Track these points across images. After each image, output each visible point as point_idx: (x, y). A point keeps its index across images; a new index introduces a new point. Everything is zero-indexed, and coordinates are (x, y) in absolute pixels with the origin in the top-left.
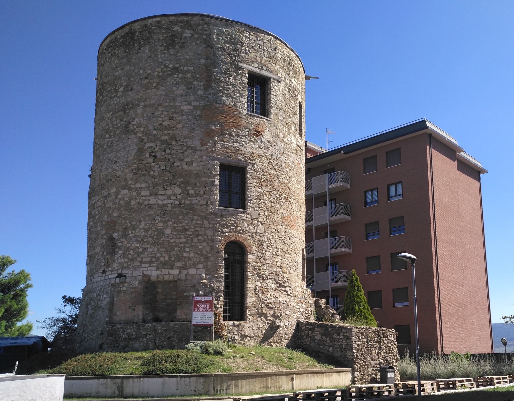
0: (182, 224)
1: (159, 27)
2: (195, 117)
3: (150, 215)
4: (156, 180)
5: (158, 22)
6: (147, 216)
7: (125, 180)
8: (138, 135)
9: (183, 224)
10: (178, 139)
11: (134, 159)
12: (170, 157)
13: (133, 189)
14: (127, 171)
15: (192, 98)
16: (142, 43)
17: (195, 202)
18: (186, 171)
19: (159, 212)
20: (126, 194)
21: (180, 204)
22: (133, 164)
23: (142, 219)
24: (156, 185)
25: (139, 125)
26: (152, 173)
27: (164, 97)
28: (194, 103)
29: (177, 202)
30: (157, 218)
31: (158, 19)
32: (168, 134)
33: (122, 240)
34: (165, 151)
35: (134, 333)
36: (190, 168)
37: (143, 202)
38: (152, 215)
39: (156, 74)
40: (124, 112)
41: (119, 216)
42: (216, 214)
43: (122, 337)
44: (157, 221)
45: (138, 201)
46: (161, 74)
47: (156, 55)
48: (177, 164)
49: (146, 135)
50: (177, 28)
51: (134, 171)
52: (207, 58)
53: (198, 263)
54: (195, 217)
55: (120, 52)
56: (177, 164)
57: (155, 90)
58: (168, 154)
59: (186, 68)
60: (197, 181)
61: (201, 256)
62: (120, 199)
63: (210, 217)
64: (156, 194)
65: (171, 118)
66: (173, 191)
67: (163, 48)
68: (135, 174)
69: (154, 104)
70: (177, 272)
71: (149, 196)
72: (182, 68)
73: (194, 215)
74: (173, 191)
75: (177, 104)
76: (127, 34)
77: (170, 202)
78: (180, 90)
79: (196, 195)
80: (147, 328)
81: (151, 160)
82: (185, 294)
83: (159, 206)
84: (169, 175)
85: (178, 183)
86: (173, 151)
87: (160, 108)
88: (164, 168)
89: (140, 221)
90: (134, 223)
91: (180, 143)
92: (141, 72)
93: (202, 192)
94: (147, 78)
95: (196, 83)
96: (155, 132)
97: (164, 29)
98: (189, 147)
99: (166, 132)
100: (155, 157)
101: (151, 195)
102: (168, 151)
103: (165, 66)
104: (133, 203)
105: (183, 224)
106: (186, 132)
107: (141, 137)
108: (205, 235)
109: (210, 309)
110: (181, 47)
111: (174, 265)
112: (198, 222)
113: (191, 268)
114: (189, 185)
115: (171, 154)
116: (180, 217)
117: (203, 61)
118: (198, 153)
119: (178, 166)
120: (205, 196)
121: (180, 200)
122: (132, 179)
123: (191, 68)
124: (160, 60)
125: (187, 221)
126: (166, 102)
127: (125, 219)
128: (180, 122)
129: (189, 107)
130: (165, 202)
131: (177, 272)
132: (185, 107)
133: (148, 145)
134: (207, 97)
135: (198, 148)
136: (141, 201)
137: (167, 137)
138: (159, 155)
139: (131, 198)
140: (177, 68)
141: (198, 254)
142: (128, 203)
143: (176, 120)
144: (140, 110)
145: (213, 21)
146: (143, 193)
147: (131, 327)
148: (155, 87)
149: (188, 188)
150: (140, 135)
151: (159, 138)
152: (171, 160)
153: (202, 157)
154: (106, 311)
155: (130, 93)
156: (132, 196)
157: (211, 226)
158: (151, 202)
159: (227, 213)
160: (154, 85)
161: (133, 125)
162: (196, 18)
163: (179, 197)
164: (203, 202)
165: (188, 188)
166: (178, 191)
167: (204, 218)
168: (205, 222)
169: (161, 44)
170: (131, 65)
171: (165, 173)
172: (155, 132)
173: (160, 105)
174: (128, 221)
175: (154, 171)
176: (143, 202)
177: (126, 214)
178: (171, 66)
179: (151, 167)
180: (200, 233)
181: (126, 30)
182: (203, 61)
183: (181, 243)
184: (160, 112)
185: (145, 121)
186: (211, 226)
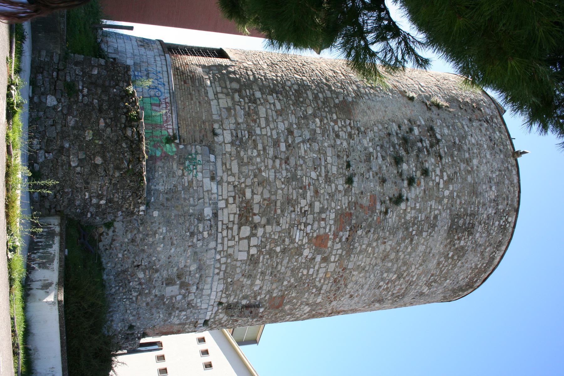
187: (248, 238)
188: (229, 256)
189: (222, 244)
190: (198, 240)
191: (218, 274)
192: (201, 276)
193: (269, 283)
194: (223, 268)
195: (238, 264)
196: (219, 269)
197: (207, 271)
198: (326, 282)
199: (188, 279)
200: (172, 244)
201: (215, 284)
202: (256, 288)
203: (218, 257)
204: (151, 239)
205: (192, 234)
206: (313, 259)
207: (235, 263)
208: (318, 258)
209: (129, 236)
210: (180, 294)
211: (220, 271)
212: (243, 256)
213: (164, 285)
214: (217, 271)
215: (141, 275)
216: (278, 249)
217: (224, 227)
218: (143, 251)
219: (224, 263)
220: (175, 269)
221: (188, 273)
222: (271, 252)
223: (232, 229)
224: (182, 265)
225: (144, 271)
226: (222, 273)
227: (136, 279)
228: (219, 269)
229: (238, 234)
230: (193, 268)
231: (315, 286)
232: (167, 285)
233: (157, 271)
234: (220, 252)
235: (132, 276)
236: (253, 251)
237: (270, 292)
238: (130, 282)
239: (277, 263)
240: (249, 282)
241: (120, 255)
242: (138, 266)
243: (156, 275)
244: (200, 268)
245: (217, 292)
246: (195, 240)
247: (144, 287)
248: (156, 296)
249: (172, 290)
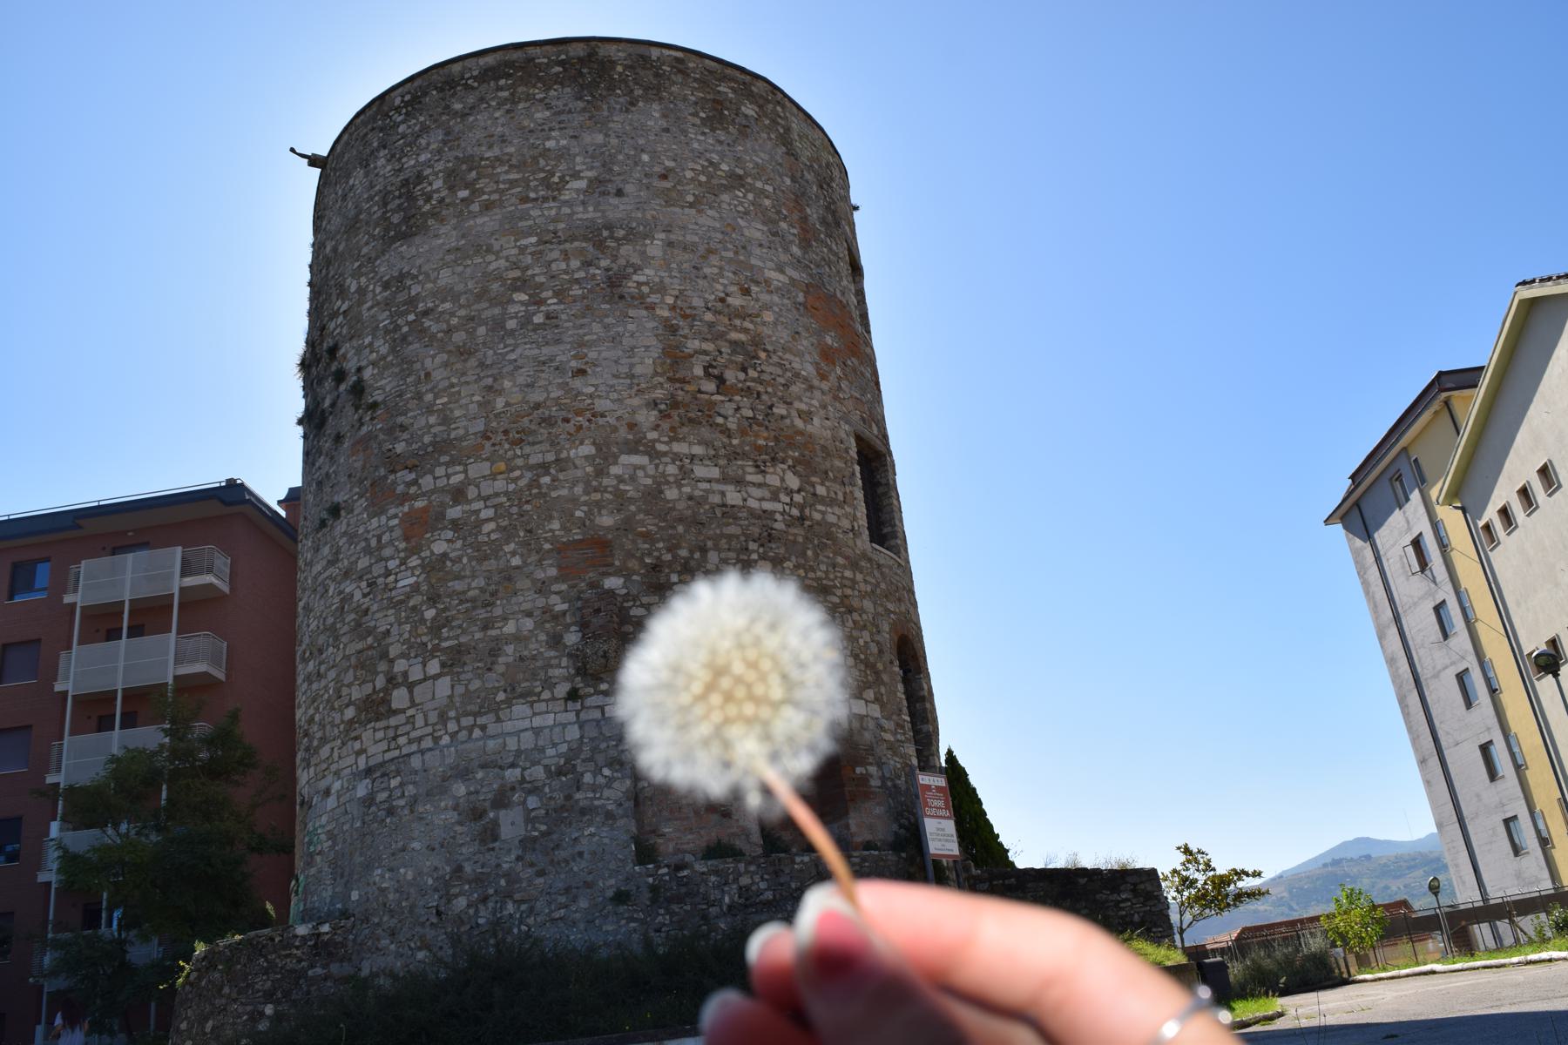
0: (814, 571)
1: (680, 71)
2: (797, 305)
3: (730, 537)
4: (735, 442)
5: (677, 59)
6: (722, 536)
7: (632, 426)
8: (658, 312)
10: (769, 348)
11: (656, 374)
12: (761, 388)
13: (665, 454)
14: (636, 401)
15: (784, 258)
16: (638, 92)
17: (831, 519)
18: (801, 433)
19: (756, 531)
20: (642, 468)
21: (802, 518)
22: (655, 387)
23: (710, 544)
24: (735, 455)
25: (661, 289)
26: (720, 420)
27: (720, 236)
28: (790, 271)
29: (795, 512)
30: (753, 546)
31: (679, 54)
32: (746, 331)
33: (645, 600)
34: (744, 370)
35: (763, 885)
36: (809, 427)
37: (705, 499)
38: (737, 537)
39: (689, 174)
40: (600, 245)
41: (627, 526)
43: (721, 900)
44: (754, 556)
45: (687, 490)
46: (703, 178)
47: (685, 132)
48: (780, 410)
49: (685, 317)
51: (663, 407)
52: (793, 180)
54: (840, 560)
55: (562, 96)
56: (780, 410)
57: (693, 211)
58: (753, 380)
59: (759, 184)
62: (620, 479)
64: (740, 482)
65: (746, 292)
66: (782, 480)
67: (698, 122)
68: (664, 415)
69: (694, 244)
71: (718, 481)
72: (749, 180)
73: (835, 554)
74: (782, 480)
75: (753, 261)
76: (580, 60)
77: (778, 507)
78: (755, 231)
79: (831, 502)
80: (801, 870)
81: (710, 386)
82: (859, 770)
83: (751, 512)
84: (765, 434)
85: (790, 462)
86: (765, 377)
87: (714, 260)
88: (750, 414)
89: (704, 550)
90: (684, 553)
91: (775, 359)
92: (645, 158)
93: (840, 497)
94: (664, 177)
95: (783, 225)
96: (709, 317)
97: (695, 80)
98: (797, 375)
99: (738, 322)
100: (721, 380)
101: (725, 479)
102: (752, 373)
103: (711, 163)
104: (671, 494)
106: (784, 335)
107: (667, 319)
108: (862, 611)
110: (740, 132)
112: (848, 574)
114: (815, 473)
115: (760, 381)
116: (809, 553)
118: (817, 394)
119: (782, 417)
121: (802, 507)
122: (656, 427)
123: (770, 189)
124: (696, 145)
125: (823, 567)
126: (726, 249)
127: (647, 536)
128: (767, 307)
129: (782, 278)
130: (768, 506)
132: (773, 275)
133: (694, 344)
135: (816, 382)
136: (697, 493)
137: (743, 337)
138: (731, 376)
139: (661, 482)
140: (740, 177)
142: (653, 495)
143: (757, 300)
144: (655, 249)
146: (700, 471)
147: (752, 868)
148: (691, 205)
149: (814, 479)
150: (666, 314)
151: (722, 336)
152: (764, 397)
154: (621, 822)
155: (614, 201)
156: (663, 474)
158: (730, 502)
160: (690, 198)
161: (639, 284)
162: (760, 84)
163: (798, 498)
165: (814, 479)
166: (793, 482)
168: (859, 577)
169: (692, 110)
170: (607, 135)
171: (755, 428)
172: (709, 317)
173: (710, 251)
174: (661, 545)
175: (726, 418)
176: (705, 499)
177: (650, 524)
178: (724, 167)
179: (712, 404)
180: (855, 603)
181: (580, 50)
182: (788, 181)
184: (716, 270)
185: (676, 281)
187: (411, 687)
188: (443, 718)
189: (420, 739)
190: (403, 795)
191: (483, 728)
192: (482, 767)
193: (514, 600)
194: (467, 721)
195: (460, 690)
196: (470, 729)
197: (473, 755)
198: (520, 462)
199: (486, 795)
200: (403, 850)
201: (508, 726)
202: (528, 624)
203: (446, 740)
204: (391, 896)
205: (391, 812)
206: (455, 525)
207: (457, 699)
208: (454, 512)
209: (384, 942)
210: (524, 803)
211: (474, 725)
212: (444, 687)
213: (497, 844)
214: (477, 733)
215: (462, 902)
216: (430, 614)
217: (393, 745)
218: (412, 908)
219: (458, 722)
220: (459, 829)
221: (472, 798)
222: (435, 629)
223: (397, 727)
224: (452, 816)
225: (449, 899)
226: (480, 721)
227: (471, 911)
228: (470, 729)
229: (403, 711)
230: (460, 789)
231: (535, 483)
232: (495, 838)
233: (459, 869)
234: (436, 740)
235: (463, 923)
236: (434, 667)
237: (542, 588)
238: (478, 925)
239: (461, 602)
240: (510, 649)
241: (421, 955)
242: (439, 913)
243: (468, 868)
244: (463, 774)
245: (535, 714)
246: (402, 802)
247: (491, 891)
248: (519, 858)
249: (511, 825)
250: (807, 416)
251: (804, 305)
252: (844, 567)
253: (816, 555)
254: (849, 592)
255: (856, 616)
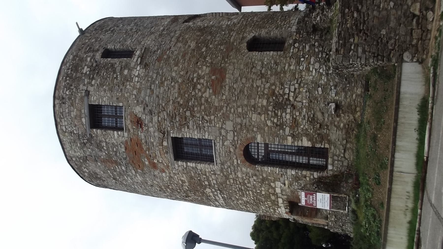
9: (236, 190)
21: (219, 190)
29: (219, 192)
42: (222, 168)
50: (86, 174)
53: (270, 185)
54: (228, 183)
60: (196, 179)
61: (263, 183)
63: (225, 173)
70: (280, 201)
73: (227, 184)
91: (169, 184)
93: (204, 176)
105: (236, 190)
108: (242, 178)
109: (315, 195)
111: (274, 201)
112: (232, 181)
113: (275, 191)
117: (99, 164)
118: (172, 175)
120: (208, 175)
129: (138, 176)
131: (280, 201)
134: (125, 164)
141: (262, 185)
145: (67, 154)
153: (175, 174)
157: (233, 173)
159: (219, 159)
164: (213, 177)
167: (227, 178)
168: (231, 176)
183: (253, 194)
186: (233, 173)
250: (182, 181)
251: (142, 170)
252: (230, 182)
253: (231, 190)
254: (238, 183)
255: (246, 182)
